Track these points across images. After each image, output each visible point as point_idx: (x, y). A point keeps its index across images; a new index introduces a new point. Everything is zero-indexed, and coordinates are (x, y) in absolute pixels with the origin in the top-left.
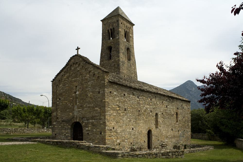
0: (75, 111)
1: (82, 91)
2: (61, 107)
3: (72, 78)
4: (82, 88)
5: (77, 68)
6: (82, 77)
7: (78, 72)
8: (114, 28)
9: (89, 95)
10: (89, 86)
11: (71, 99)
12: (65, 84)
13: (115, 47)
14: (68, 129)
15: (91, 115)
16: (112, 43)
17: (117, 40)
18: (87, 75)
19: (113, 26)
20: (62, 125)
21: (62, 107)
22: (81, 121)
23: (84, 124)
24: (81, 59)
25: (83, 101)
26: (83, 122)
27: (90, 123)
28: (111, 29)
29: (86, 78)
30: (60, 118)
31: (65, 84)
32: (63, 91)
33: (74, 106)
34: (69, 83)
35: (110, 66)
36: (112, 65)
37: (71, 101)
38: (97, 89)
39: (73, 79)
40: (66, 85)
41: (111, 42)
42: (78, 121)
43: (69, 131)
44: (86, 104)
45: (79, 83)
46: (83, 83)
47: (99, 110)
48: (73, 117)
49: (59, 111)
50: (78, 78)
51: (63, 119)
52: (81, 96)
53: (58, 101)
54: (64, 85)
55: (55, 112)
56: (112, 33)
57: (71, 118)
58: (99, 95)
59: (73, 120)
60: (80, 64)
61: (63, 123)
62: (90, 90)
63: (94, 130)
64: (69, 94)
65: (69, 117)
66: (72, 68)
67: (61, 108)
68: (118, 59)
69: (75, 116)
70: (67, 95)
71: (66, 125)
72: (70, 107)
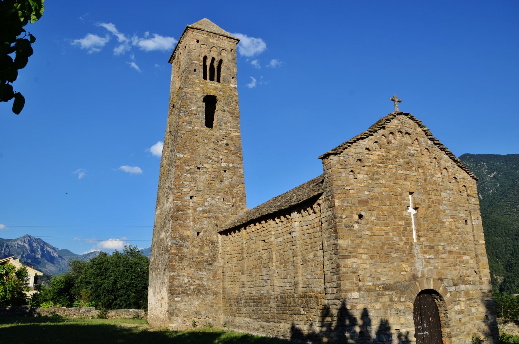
0: (416, 260)
1: (428, 209)
2: (368, 242)
3: (397, 168)
4: (426, 200)
5: (410, 147)
6: (425, 175)
7: (413, 158)
8: (221, 62)
9: (447, 223)
10: (445, 202)
11: (400, 223)
12: (376, 176)
13: (227, 104)
14: (404, 313)
15: (457, 272)
16: (221, 93)
17: (231, 90)
18: (436, 174)
19: (220, 54)
20: (386, 299)
21: (374, 243)
22: (441, 288)
23: (448, 295)
24: (419, 129)
25: (435, 236)
26: (446, 290)
27: (462, 292)
28: (213, 59)
29: (434, 178)
30: (368, 279)
31: (376, 176)
32: (372, 194)
33: (412, 245)
34: (390, 177)
35: (215, 144)
36: (220, 143)
37: (402, 229)
38: (461, 212)
39: (399, 172)
40: (381, 181)
41: (216, 88)
42: (432, 288)
43: (411, 317)
44: (442, 244)
45: (420, 187)
46: (428, 189)
47: (471, 261)
48: (414, 277)
49: (365, 254)
50: (412, 171)
51: (379, 282)
52: (427, 221)
53: (357, 222)
54: (372, 179)
55: (354, 257)
56: (206, 66)
57: (407, 279)
58: (468, 228)
59: (417, 284)
60: (416, 139)
61: (387, 292)
62: (447, 212)
63: (473, 310)
64: (391, 207)
65: (401, 276)
66: (393, 141)
67: (371, 246)
68: (237, 134)
69: (419, 275)
70: (384, 207)
71: (400, 298)
72: (401, 246)
